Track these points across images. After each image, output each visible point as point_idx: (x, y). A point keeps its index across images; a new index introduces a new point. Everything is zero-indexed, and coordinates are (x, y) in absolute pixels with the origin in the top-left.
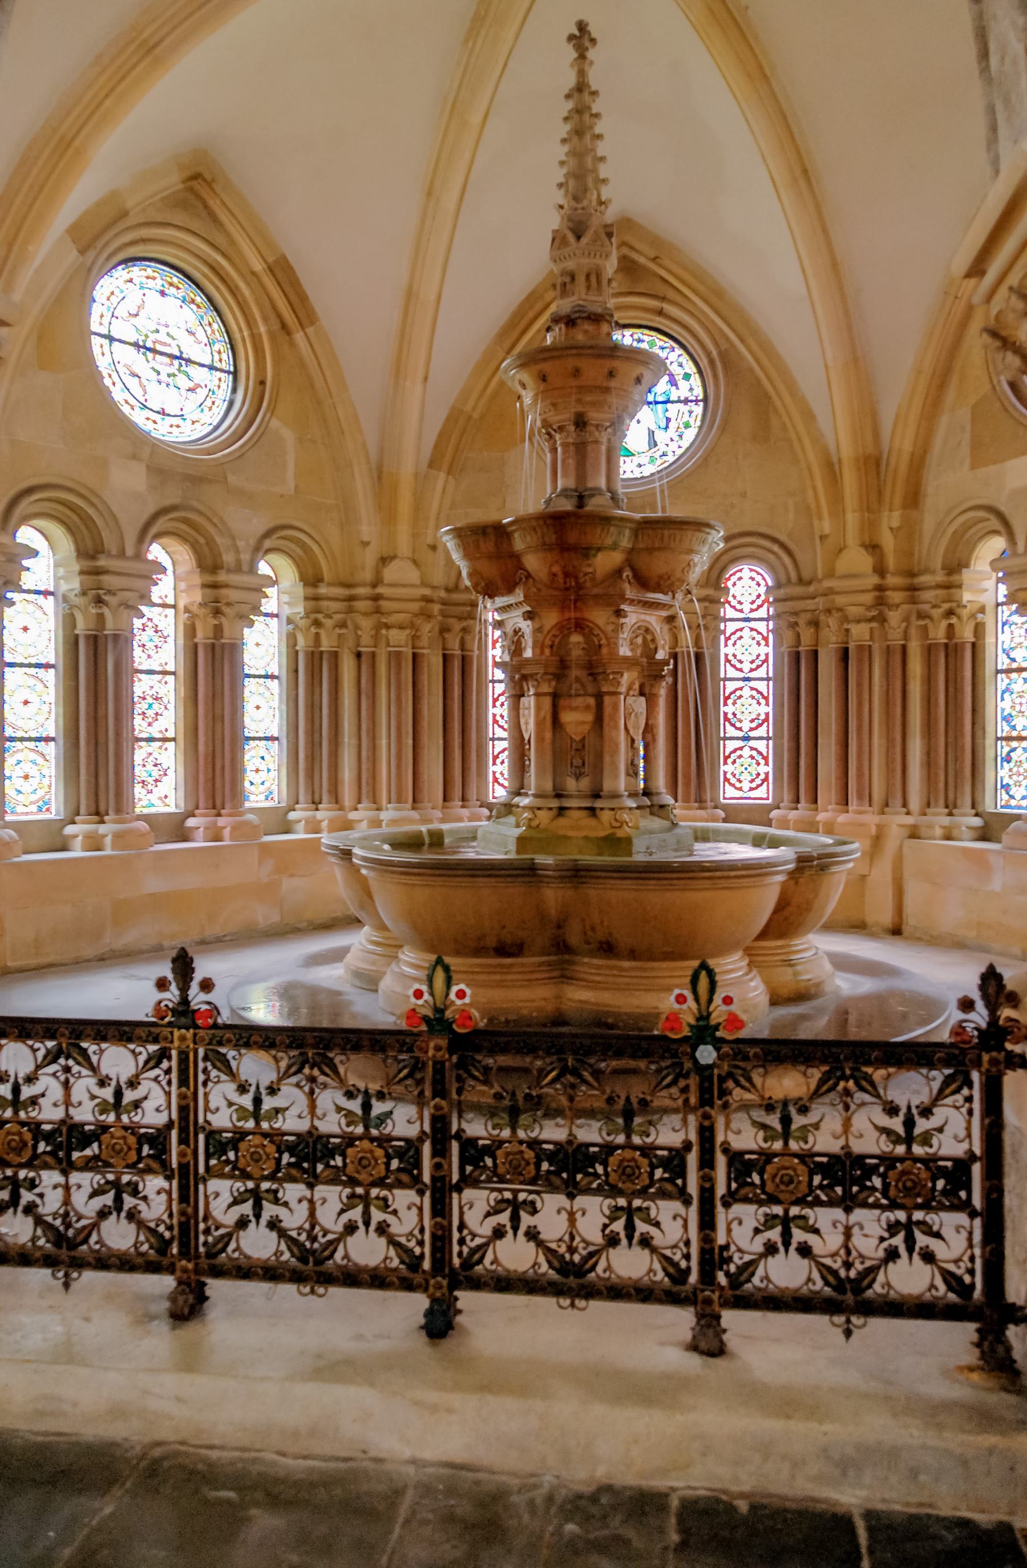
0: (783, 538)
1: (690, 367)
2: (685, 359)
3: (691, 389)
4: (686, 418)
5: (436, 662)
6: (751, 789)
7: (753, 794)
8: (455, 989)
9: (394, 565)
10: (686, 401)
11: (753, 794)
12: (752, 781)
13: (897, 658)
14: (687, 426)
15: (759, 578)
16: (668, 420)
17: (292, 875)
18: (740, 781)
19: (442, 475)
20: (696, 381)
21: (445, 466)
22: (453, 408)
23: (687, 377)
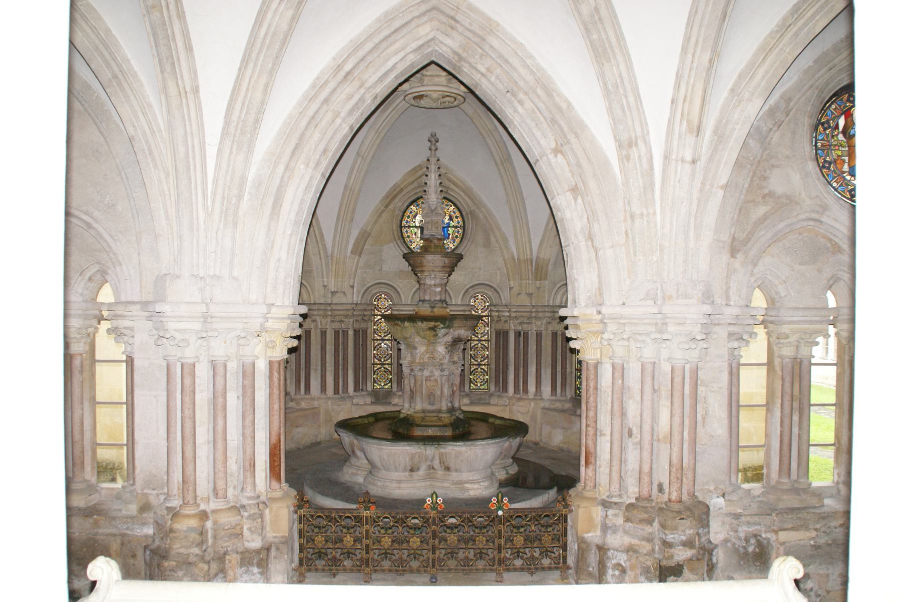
0: (495, 286)
1: (458, 214)
2: (456, 210)
3: (458, 223)
4: (456, 234)
5: (351, 333)
6: (481, 385)
7: (482, 387)
8: (438, 499)
9: (338, 295)
10: (456, 227)
11: (482, 387)
12: (481, 382)
13: (539, 336)
14: (457, 237)
15: (485, 299)
16: (449, 234)
17: (297, 427)
18: (477, 382)
19: (357, 257)
20: (460, 219)
21: (358, 253)
22: (362, 229)
23: (457, 217)
